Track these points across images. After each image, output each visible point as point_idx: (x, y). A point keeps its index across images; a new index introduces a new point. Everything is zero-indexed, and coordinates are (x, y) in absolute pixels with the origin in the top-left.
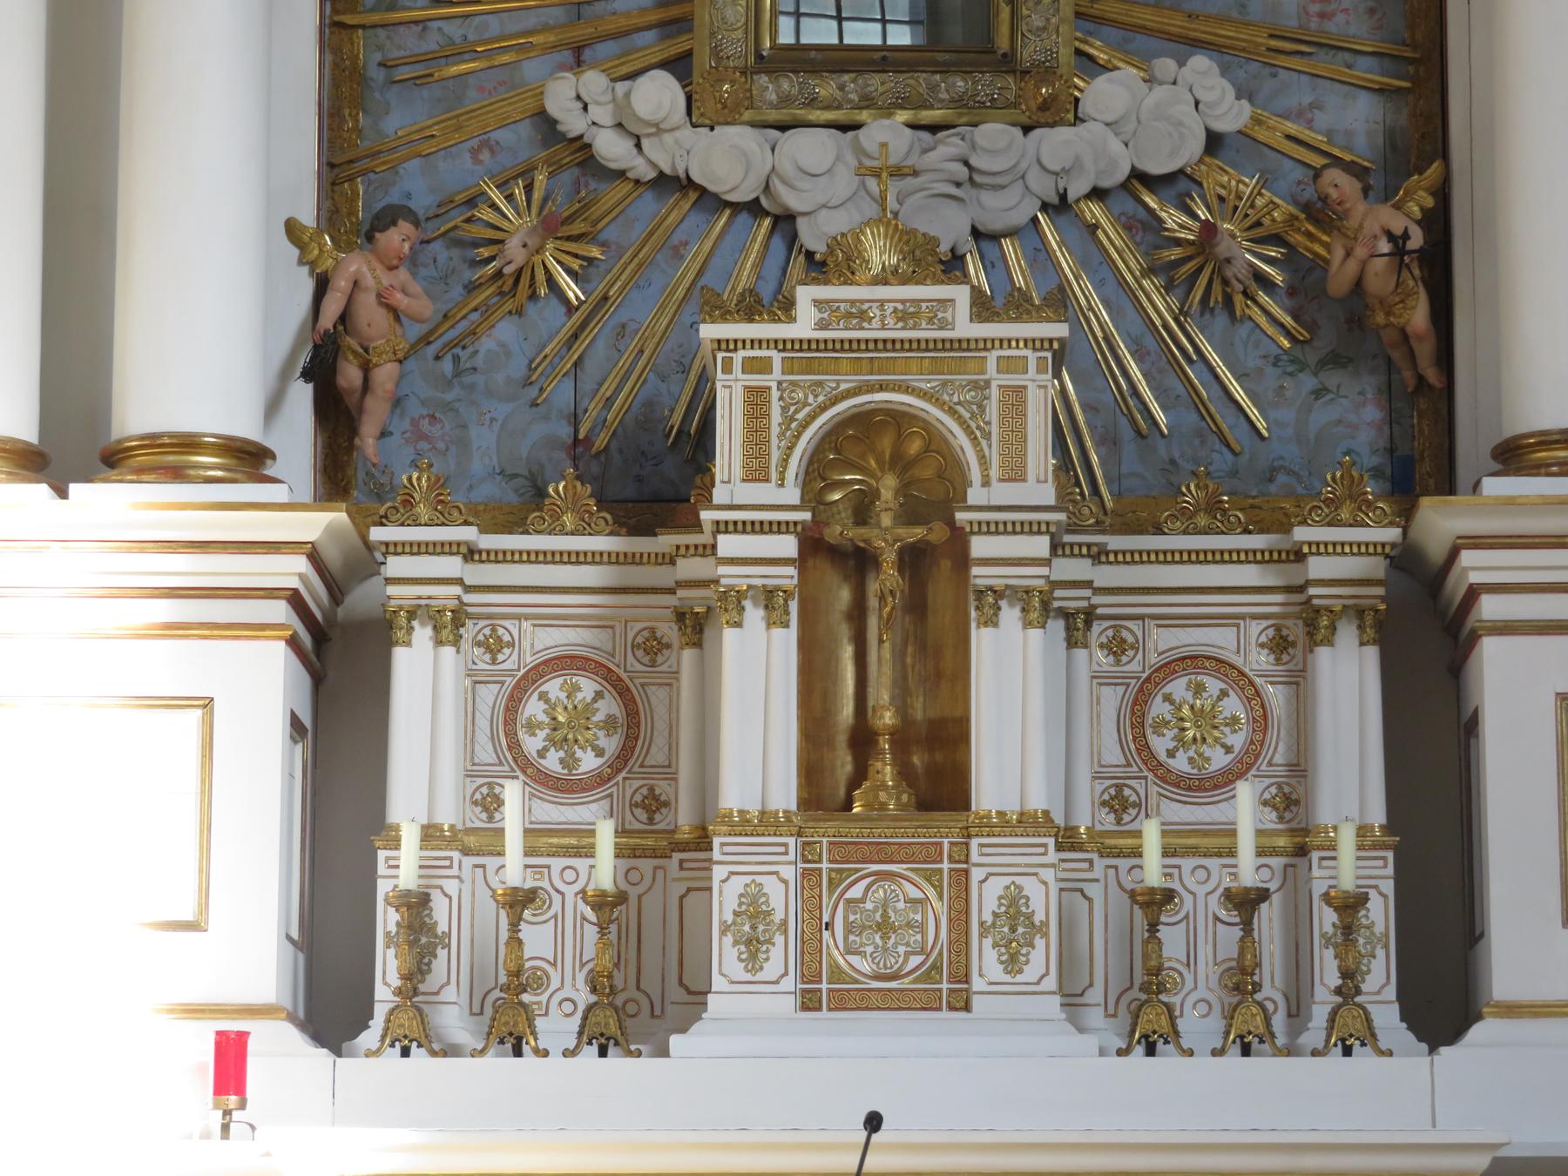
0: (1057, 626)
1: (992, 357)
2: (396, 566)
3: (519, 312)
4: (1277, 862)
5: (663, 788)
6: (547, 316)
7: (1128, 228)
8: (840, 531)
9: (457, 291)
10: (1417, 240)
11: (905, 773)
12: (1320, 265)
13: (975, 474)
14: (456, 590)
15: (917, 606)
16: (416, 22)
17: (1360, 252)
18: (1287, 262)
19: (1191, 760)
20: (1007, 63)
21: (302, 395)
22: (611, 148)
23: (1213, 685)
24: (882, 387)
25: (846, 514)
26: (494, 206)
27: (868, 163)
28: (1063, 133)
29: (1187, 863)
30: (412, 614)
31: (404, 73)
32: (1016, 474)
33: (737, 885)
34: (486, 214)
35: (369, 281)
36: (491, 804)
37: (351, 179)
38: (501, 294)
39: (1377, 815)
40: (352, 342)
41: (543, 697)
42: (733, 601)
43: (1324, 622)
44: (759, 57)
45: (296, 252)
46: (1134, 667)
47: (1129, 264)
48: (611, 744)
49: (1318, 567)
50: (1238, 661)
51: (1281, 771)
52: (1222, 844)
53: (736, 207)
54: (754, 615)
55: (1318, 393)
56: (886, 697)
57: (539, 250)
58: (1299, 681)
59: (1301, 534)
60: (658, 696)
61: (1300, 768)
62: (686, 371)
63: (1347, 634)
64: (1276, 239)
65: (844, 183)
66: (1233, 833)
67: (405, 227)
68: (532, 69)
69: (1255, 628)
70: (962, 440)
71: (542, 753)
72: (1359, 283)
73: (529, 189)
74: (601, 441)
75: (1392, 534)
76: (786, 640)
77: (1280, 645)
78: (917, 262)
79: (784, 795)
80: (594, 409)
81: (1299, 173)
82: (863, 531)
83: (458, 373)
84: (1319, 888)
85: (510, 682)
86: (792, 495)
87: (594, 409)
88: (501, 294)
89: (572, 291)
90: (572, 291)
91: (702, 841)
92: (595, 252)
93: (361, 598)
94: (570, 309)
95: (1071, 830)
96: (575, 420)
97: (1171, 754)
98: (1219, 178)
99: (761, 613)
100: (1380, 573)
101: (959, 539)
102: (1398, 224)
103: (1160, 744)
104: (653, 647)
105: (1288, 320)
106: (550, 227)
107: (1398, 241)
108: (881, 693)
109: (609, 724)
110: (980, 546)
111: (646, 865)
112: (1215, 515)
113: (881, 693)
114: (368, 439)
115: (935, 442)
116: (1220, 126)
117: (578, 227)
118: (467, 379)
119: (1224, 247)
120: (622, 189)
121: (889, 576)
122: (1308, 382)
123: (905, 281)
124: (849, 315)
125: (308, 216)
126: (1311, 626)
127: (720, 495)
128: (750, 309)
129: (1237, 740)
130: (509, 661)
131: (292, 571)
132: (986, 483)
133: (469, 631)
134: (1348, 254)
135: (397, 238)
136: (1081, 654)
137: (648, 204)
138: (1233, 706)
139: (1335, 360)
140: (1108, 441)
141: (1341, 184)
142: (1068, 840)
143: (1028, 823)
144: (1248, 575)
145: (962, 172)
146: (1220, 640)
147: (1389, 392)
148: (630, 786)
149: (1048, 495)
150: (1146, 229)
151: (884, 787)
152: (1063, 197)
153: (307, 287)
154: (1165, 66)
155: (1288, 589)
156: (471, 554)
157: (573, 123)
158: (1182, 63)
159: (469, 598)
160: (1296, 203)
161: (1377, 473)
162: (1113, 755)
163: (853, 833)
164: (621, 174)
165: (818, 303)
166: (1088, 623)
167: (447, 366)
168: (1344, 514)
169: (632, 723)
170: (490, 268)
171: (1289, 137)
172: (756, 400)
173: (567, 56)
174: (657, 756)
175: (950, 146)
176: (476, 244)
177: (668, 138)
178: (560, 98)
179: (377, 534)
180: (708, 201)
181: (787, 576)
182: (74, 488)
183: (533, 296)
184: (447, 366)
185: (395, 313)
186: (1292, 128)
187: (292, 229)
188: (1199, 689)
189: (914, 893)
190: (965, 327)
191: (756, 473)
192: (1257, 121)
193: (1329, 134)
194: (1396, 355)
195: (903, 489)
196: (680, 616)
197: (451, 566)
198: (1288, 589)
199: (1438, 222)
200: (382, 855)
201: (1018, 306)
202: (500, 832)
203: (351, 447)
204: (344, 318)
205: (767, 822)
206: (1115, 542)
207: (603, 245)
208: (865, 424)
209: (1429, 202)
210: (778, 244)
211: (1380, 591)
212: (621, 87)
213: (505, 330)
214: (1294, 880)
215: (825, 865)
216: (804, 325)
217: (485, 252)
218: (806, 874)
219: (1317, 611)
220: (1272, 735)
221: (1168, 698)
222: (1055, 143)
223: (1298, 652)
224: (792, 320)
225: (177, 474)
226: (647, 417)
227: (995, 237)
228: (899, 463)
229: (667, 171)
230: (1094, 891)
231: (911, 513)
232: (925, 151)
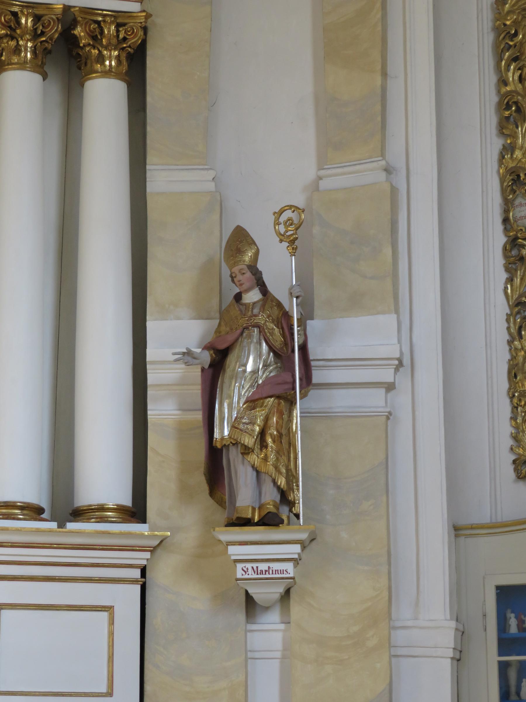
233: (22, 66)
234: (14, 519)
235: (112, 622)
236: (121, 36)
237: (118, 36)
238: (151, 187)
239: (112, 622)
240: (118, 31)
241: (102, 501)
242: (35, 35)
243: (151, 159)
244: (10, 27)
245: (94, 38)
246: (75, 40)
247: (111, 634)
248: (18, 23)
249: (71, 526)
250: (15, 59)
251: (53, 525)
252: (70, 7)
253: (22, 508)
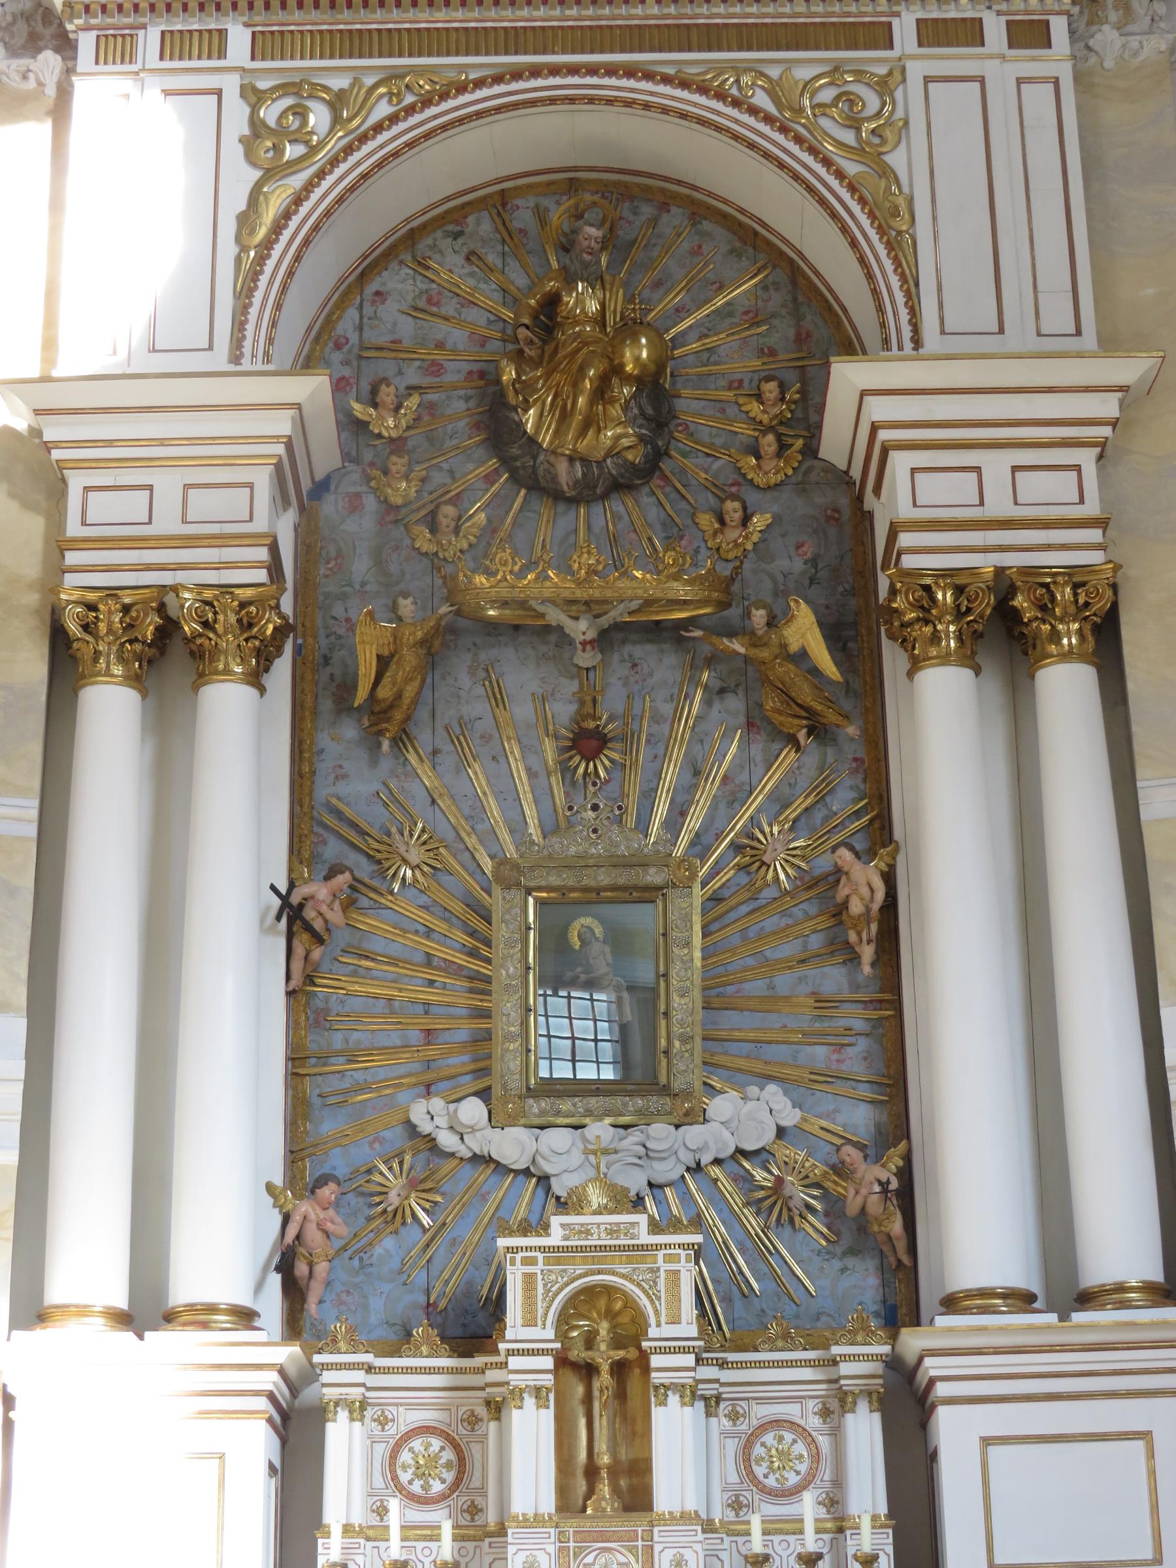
0: (700, 1405)
1: (660, 1254)
2: (328, 1377)
3: (396, 1232)
4: (827, 1537)
5: (479, 1501)
6: (411, 1234)
7: (735, 1180)
8: (578, 1354)
9: (362, 1221)
10: (894, 1184)
11: (616, 1490)
12: (842, 1199)
13: (652, 1320)
14: (362, 1390)
15: (621, 1395)
16: (339, 1072)
17: (864, 1191)
18: (826, 1196)
19: (777, 1479)
20: (666, 1090)
21: (275, 1281)
22: (447, 1140)
23: (788, 1437)
24: (599, 1272)
25: (580, 1344)
26: (381, 1173)
27: (590, 1147)
28: (697, 1128)
29: (776, 1539)
30: (337, 1404)
31: (332, 1100)
32: (675, 1320)
33: (522, 1556)
34: (377, 1178)
35: (312, 1216)
36: (382, 1511)
37: (302, 1159)
38: (386, 1222)
39: (883, 1509)
40: (302, 1250)
41: (411, 1450)
42: (518, 1394)
43: (850, 1399)
44: (528, 1089)
45: (271, 1200)
46: (744, 1427)
47: (736, 1200)
48: (450, 1476)
49: (845, 1369)
50: (802, 1422)
51: (828, 1484)
52: (795, 1527)
53: (517, 1172)
54: (529, 1401)
55: (843, 1270)
56: (604, 1447)
57: (407, 1198)
58: (836, 1433)
59: (836, 1350)
60: (476, 1448)
61: (839, 1482)
62: (490, 1264)
63: (863, 1406)
64: (817, 1185)
65: (576, 1158)
66: (802, 1521)
67: (332, 1186)
68: (402, 1097)
69: (811, 1404)
70: (644, 1301)
71: (410, 1482)
72: (863, 1210)
73: (401, 1163)
74: (442, 1304)
75: (886, 1349)
76: (547, 1418)
77: (825, 1413)
78: (618, 1202)
79: (548, 1504)
80: (438, 1286)
81: (829, 1148)
82: (590, 1353)
83: (362, 1267)
84: (851, 1551)
85: (392, 1442)
86: (550, 1333)
87: (438, 1286)
88: (386, 1222)
89: (426, 1220)
90: (426, 1220)
91: (502, 1531)
92: (439, 1199)
93: (309, 1394)
94: (425, 1231)
95: (710, 1521)
96: (428, 1293)
97: (766, 1476)
98: (785, 1152)
99: (533, 1400)
100: (880, 1372)
101: (644, 1357)
102: (884, 1175)
103: (759, 1471)
104: (473, 1420)
105: (825, 1230)
106: (414, 1184)
107: (884, 1185)
108: (601, 1445)
109: (448, 1465)
110: (656, 1361)
111: (470, 1545)
112: (787, 1340)
113: (601, 1445)
114: (312, 1305)
115: (630, 1303)
116: (783, 1123)
117: (429, 1185)
118: (368, 1270)
119: (787, 1191)
120: (454, 1163)
121: (605, 1379)
122: (837, 1264)
123: (611, 1212)
125: (278, 1181)
126: (842, 1401)
127: (509, 1334)
128: (525, 1229)
129: (803, 1468)
130: (391, 1429)
131: (269, 1380)
132: (659, 1325)
133: (369, 1413)
134: (857, 1193)
135: (328, 1192)
136: (714, 1420)
137: (467, 1171)
138: (800, 1448)
139: (852, 1252)
140: (727, 1300)
141: (851, 1154)
142: (709, 1527)
143: (686, 1518)
144: (807, 1374)
145: (642, 1151)
146: (792, 1411)
147: (882, 1269)
148: (460, 1499)
149: (693, 1331)
150: (745, 1181)
151: (604, 1498)
152: (698, 1164)
153: (278, 1220)
154: (753, 1090)
155: (829, 1381)
156: (370, 1369)
157: (425, 1127)
158: (762, 1089)
159: (368, 1394)
160: (827, 1165)
161: (877, 1314)
162: (733, 1478)
163: (587, 1526)
164: (453, 1155)
165: (562, 1225)
166: (718, 1403)
167: (356, 1262)
168: (859, 1338)
169: (461, 1464)
170: (380, 1208)
171: (822, 1128)
172: (529, 1280)
173: (422, 1089)
174: (476, 1483)
175: (635, 1136)
176: (372, 1195)
177: (478, 1134)
178: (418, 1113)
179: (317, 1359)
180: (501, 1169)
181: (548, 1380)
182: (147, 1334)
183: (404, 1223)
184: (356, 1262)
185: (327, 1234)
186: (824, 1124)
187: (270, 1187)
188: (781, 1439)
189: (622, 1559)
190: (645, 1238)
191: (530, 1322)
192: (804, 1120)
193: (844, 1126)
194: (885, 1249)
195: (613, 1328)
196: (488, 1403)
197: (359, 1376)
198: (829, 1381)
199: (906, 1174)
200: (320, 1541)
201: (675, 1225)
202: (387, 1527)
203: (302, 1310)
204: (298, 1237)
205: (538, 1520)
206: (732, 1357)
207: (443, 1194)
208: (590, 1292)
209: (901, 1163)
210: (540, 1192)
211: (880, 1381)
212: (452, 1107)
213: (389, 1243)
214: (837, 1547)
215: (572, 1544)
216: (555, 1238)
217: (377, 1199)
219: (846, 1393)
220: (823, 1463)
221: (763, 1445)
222: (694, 1134)
223: (835, 1416)
224: (548, 1235)
225: (205, 1326)
226: (469, 1291)
227: (661, 1187)
228: (610, 1314)
229: (478, 1152)
230: (724, 1556)
231: (617, 1343)
232: (621, 1140)
233: (945, 659)
234: (994, 1313)
235: (1151, 1454)
236: (1081, 601)
237: (1076, 601)
238: (1145, 814)
239: (1151, 1454)
240: (1076, 595)
241: (1119, 1278)
242: (959, 614)
243: (1143, 772)
244: (922, 607)
245: (1043, 608)
246: (1016, 614)
247: (1152, 1473)
248: (933, 599)
249: (1078, 1317)
250: (933, 652)
251: (1052, 1318)
252: (1004, 569)
253: (1004, 1296)
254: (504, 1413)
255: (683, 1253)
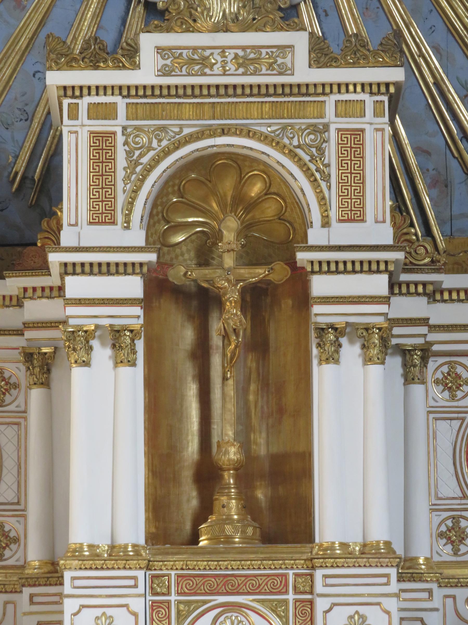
24: (224, 132)
62: (29, 119)
78: (257, 9)
82: (207, 272)
99: (108, 352)
124: (191, 62)
132: (326, 224)
151: (229, 520)
165: (160, 50)
166: (424, 360)
215: (173, 598)
218: (155, 606)
224: (136, 66)
254: (55, 373)
255: (369, 100)
